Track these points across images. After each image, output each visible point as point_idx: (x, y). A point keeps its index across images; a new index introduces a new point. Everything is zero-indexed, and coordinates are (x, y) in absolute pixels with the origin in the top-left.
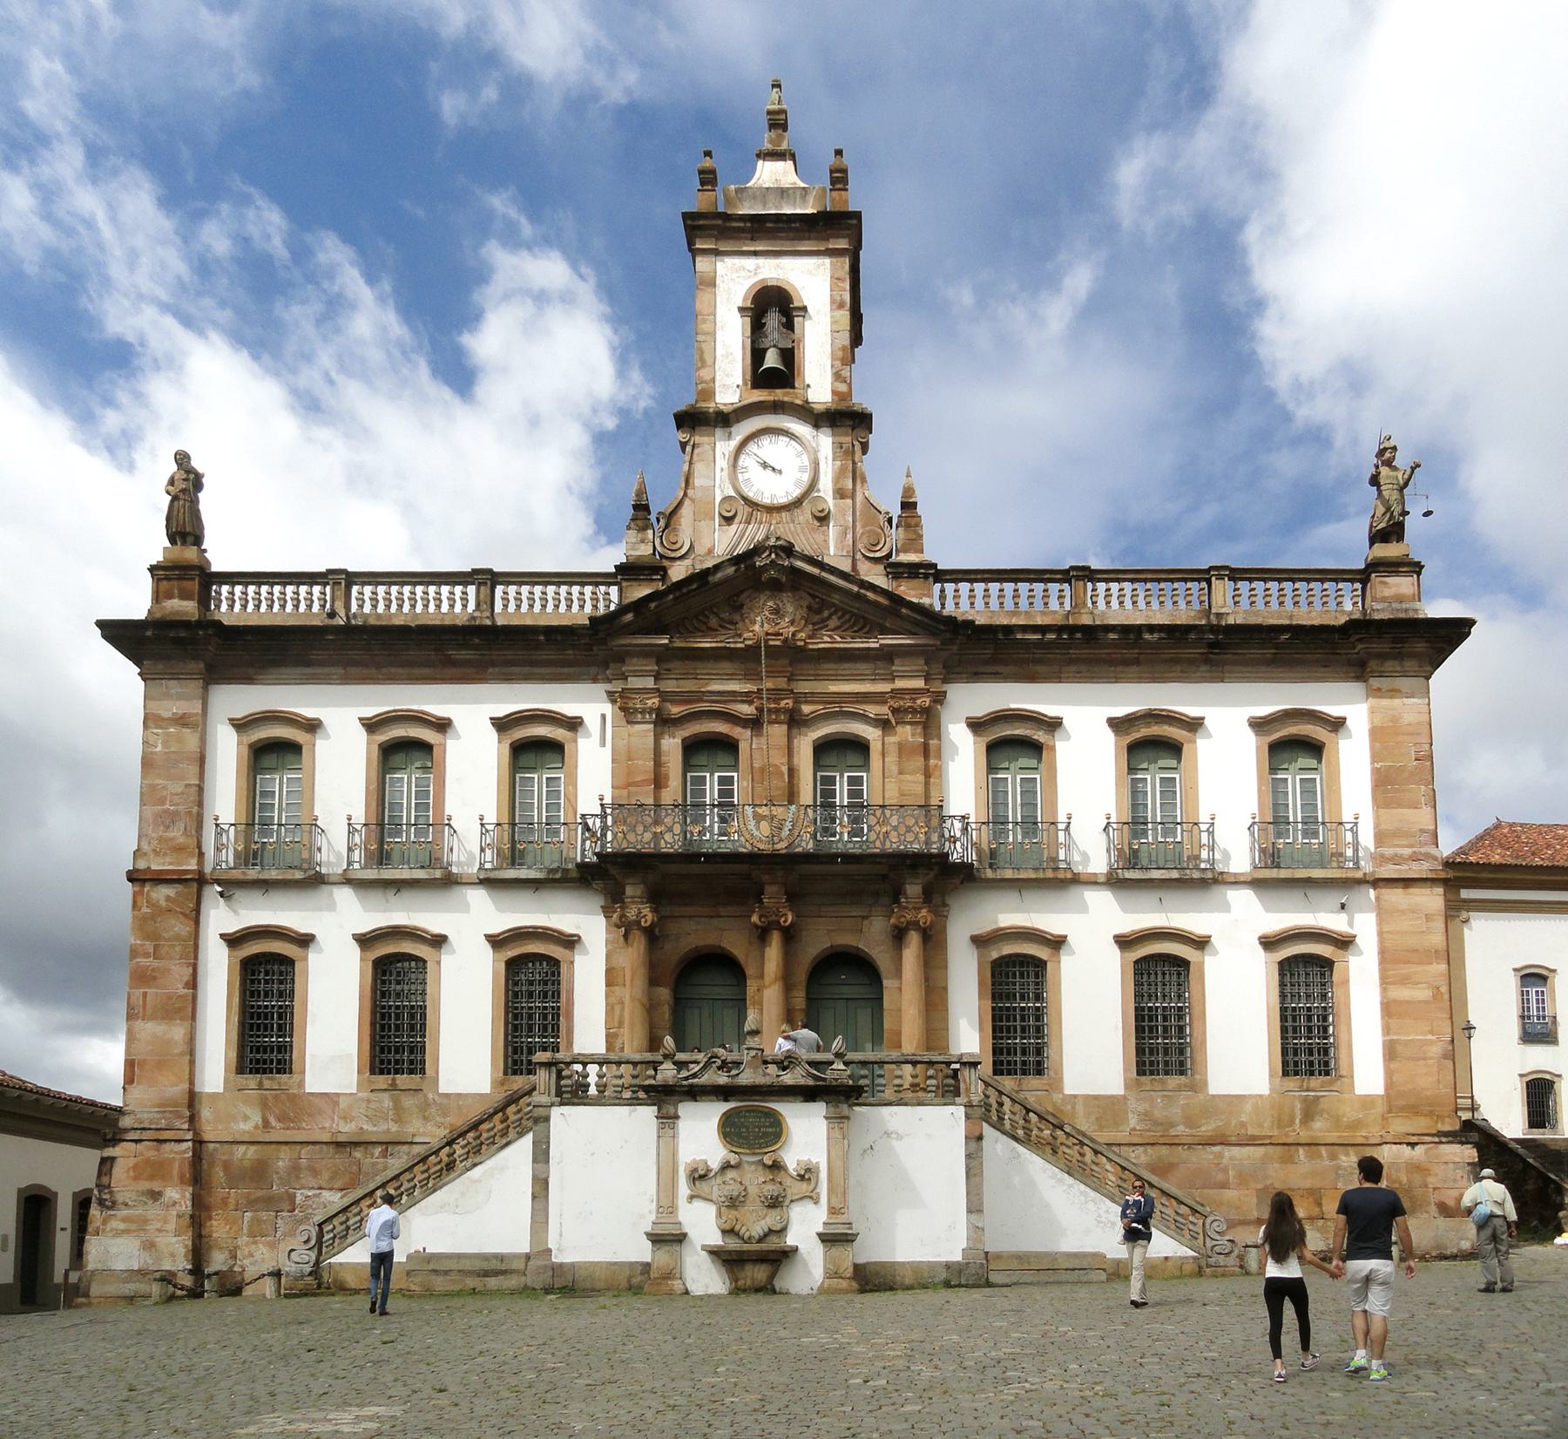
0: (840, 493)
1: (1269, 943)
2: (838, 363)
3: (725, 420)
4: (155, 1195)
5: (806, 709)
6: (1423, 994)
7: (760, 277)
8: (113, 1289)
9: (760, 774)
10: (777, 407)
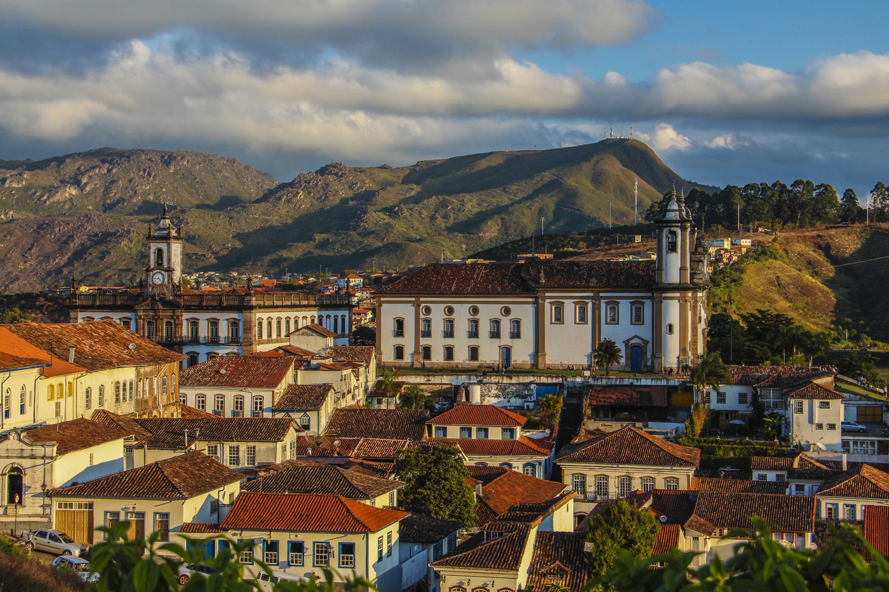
0: (169, 283)
3: (152, 270)
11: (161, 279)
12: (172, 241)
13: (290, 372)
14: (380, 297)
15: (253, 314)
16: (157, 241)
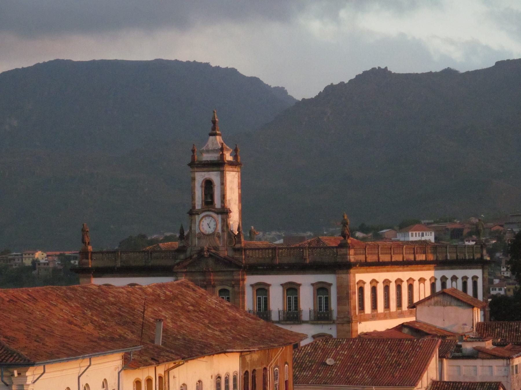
0: (223, 231)
2: (222, 199)
3: (198, 214)
7: (204, 178)
11: (212, 225)
12: (227, 168)
13: (433, 363)
15: (352, 275)
16: (205, 169)
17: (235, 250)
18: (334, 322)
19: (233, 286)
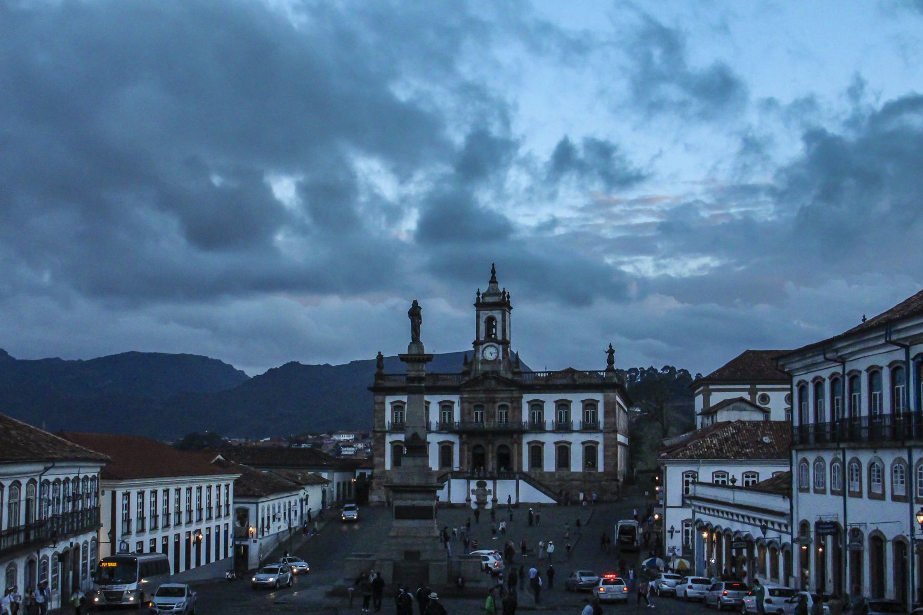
0: (503, 357)
1: (583, 443)
3: (482, 343)
4: (380, 488)
5: (496, 400)
6: (610, 453)
8: (374, 504)
9: (488, 412)
10: (493, 342)
14: (709, 384)
16: (488, 308)
17: (514, 373)
18: (601, 432)
19: (512, 402)
